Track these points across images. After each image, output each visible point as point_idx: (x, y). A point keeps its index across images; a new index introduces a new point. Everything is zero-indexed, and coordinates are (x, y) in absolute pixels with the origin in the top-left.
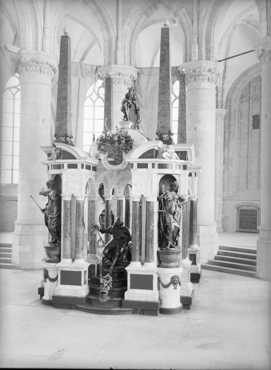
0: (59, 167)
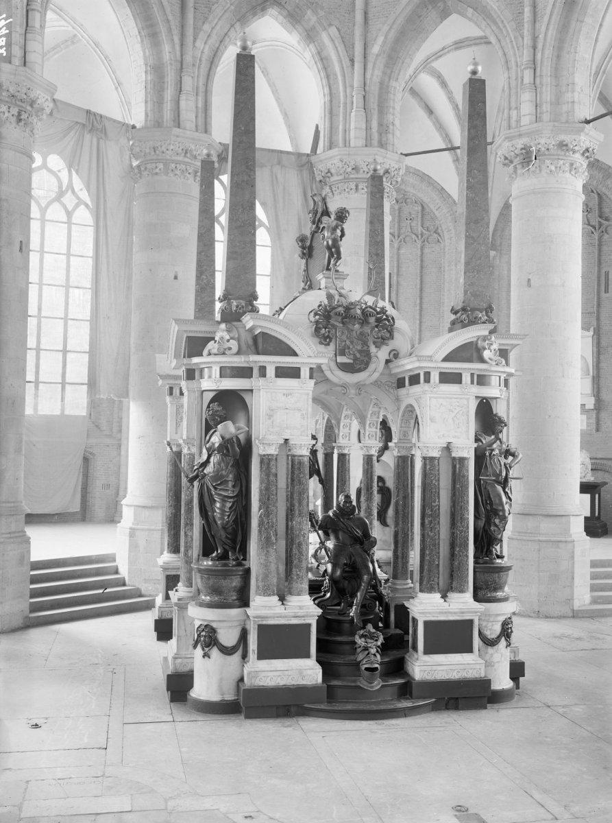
0: (245, 372)
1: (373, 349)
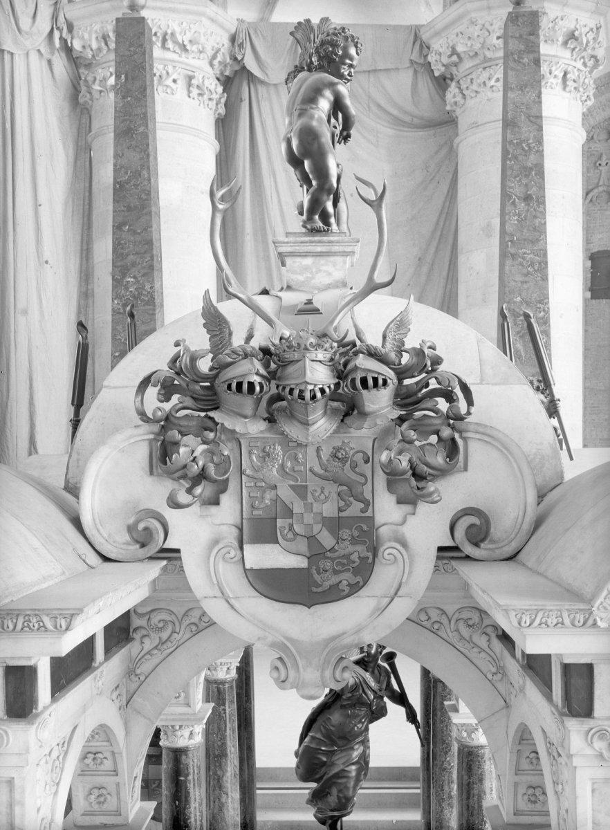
1: (386, 509)
